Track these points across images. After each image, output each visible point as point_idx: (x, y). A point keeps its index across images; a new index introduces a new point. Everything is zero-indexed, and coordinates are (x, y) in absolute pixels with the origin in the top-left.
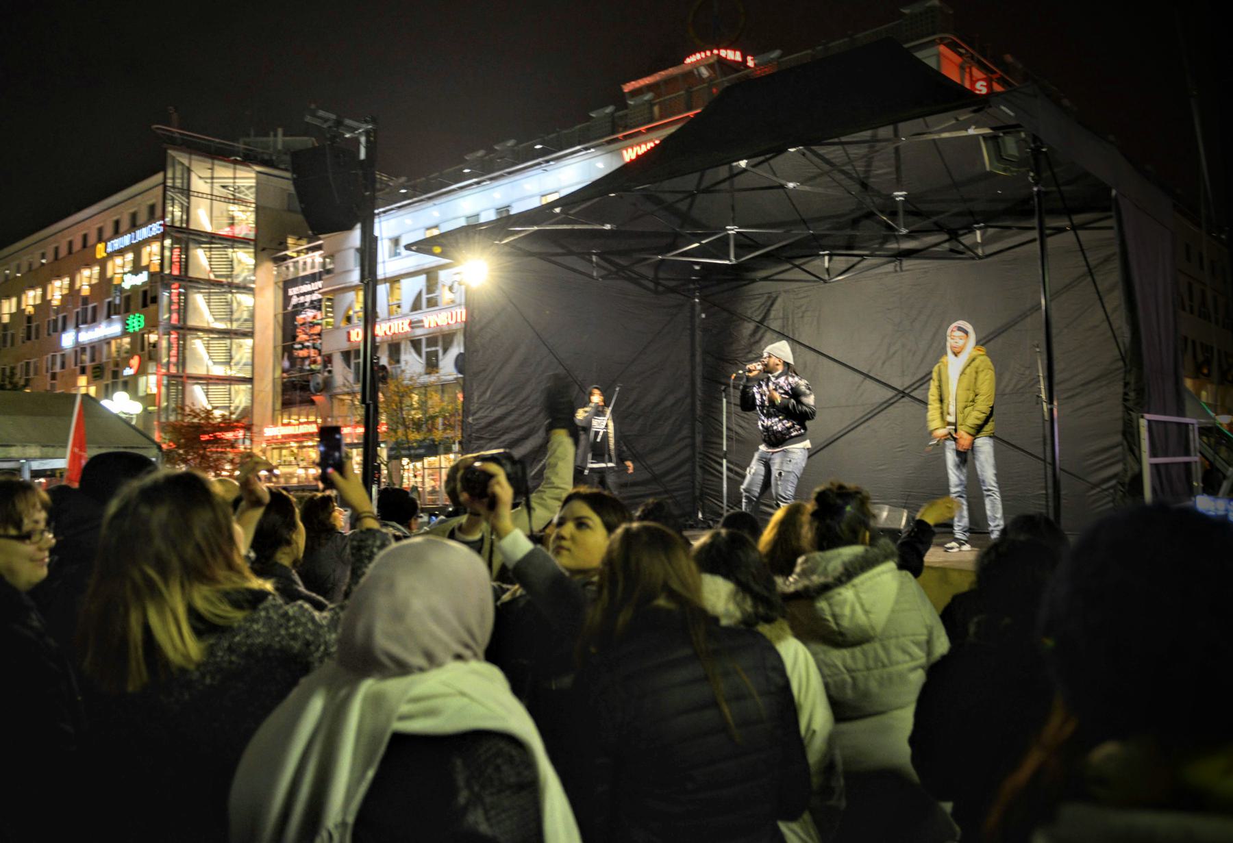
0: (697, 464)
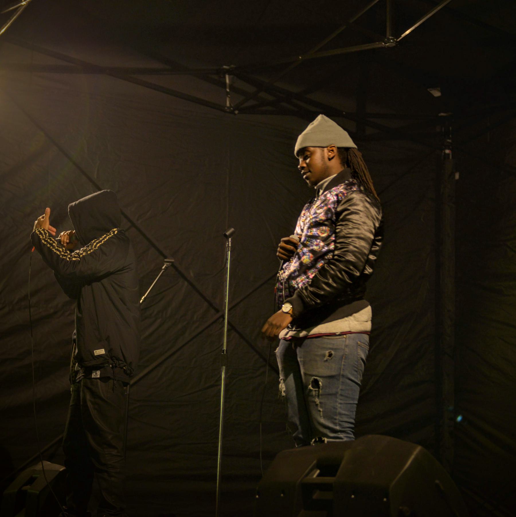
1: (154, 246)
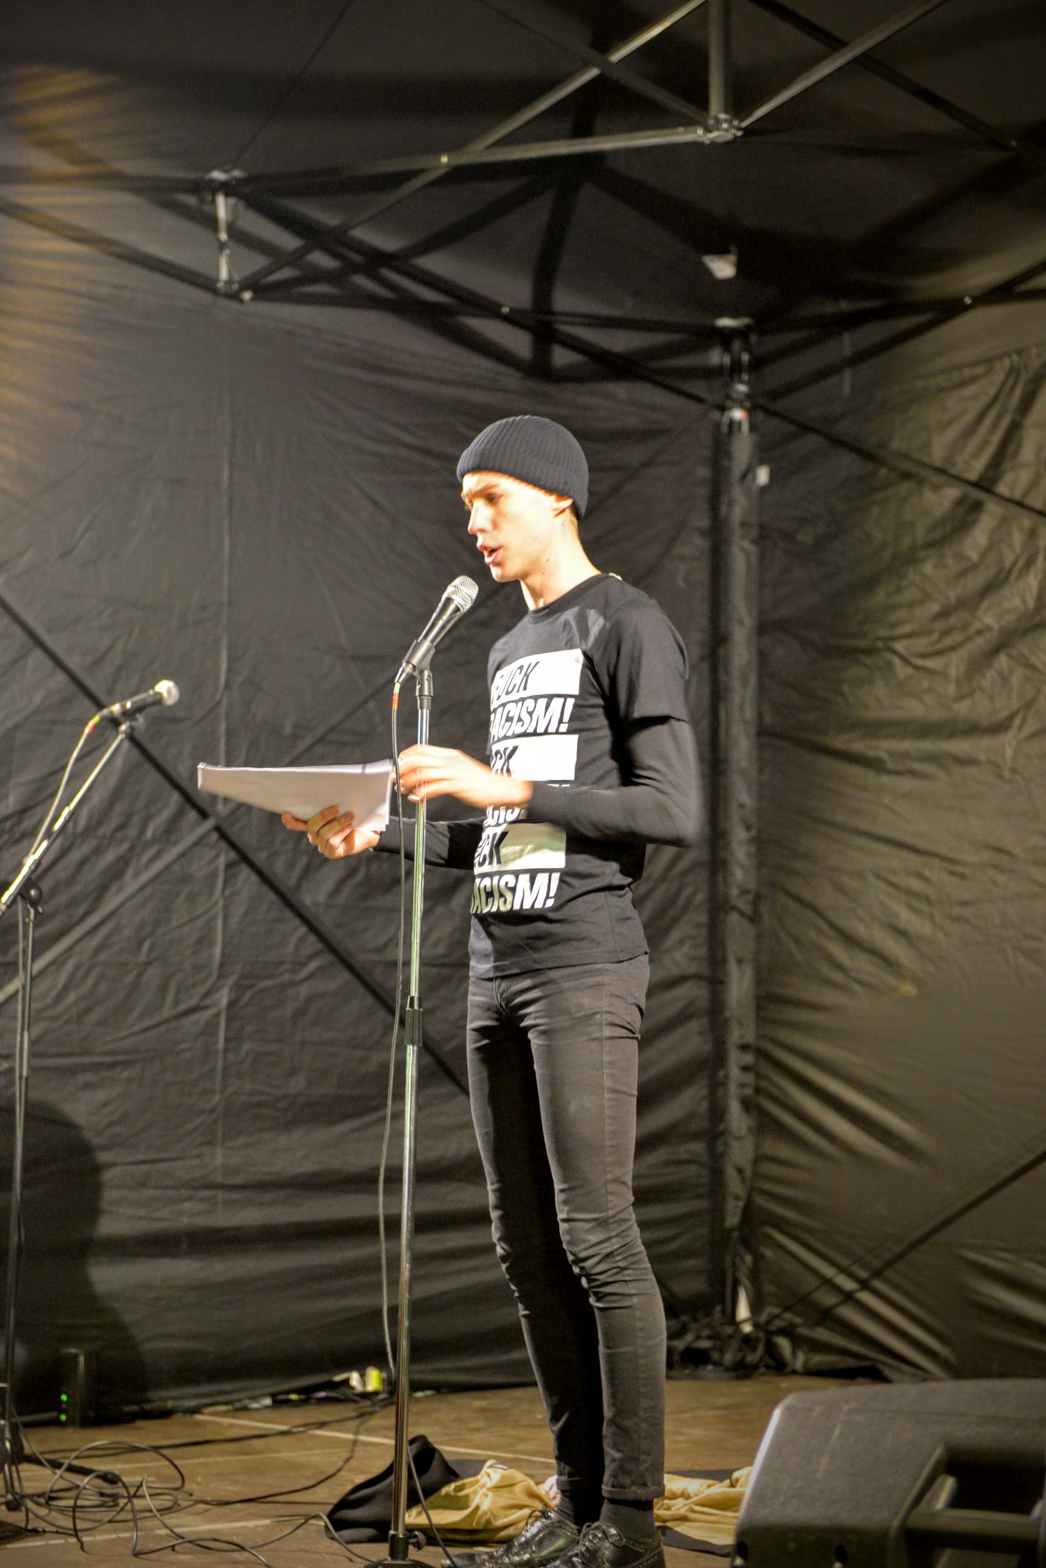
0: (733, 1089)
1: (38, 642)
